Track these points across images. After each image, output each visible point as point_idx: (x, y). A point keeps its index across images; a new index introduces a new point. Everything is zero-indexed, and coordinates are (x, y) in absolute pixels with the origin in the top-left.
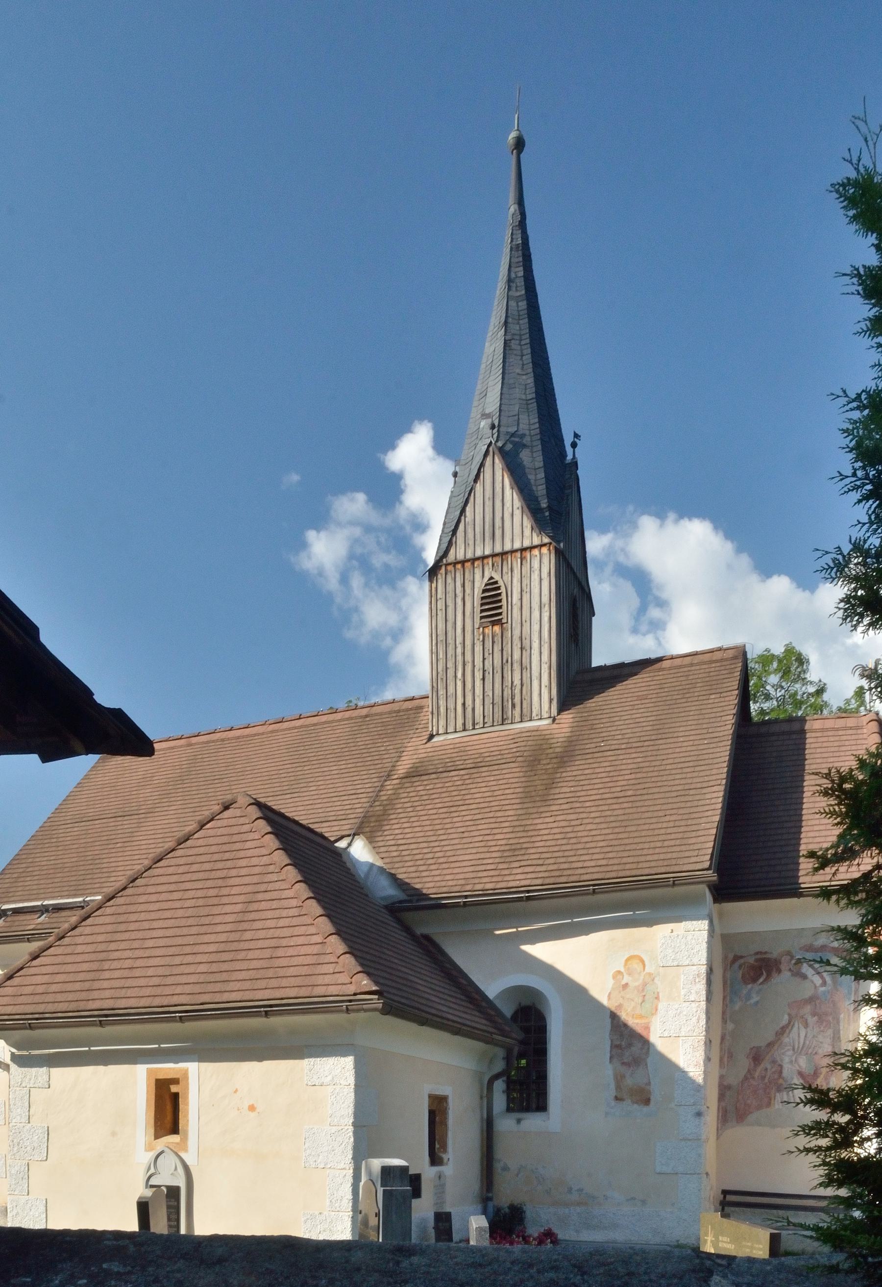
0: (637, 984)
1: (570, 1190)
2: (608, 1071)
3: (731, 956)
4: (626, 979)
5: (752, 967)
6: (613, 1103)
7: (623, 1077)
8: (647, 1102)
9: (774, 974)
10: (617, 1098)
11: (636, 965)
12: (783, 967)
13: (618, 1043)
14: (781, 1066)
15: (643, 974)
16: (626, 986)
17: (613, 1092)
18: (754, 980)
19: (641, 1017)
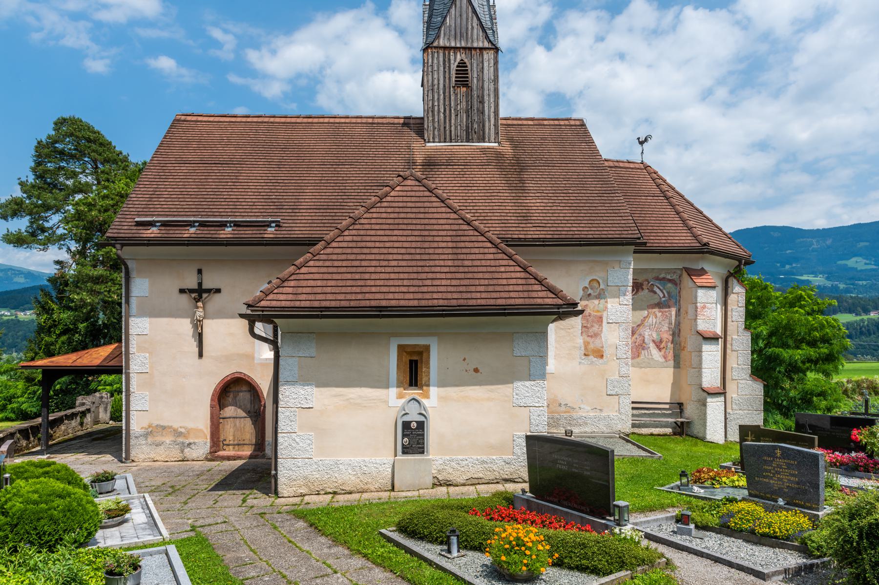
0: (596, 294)
1: (560, 405)
2: (580, 341)
4: (590, 291)
6: (583, 357)
7: (589, 343)
8: (602, 356)
9: (640, 290)
10: (585, 355)
11: (595, 284)
12: (644, 287)
13: (586, 325)
14: (644, 337)
15: (599, 289)
16: (590, 295)
17: (583, 353)
19: (598, 311)
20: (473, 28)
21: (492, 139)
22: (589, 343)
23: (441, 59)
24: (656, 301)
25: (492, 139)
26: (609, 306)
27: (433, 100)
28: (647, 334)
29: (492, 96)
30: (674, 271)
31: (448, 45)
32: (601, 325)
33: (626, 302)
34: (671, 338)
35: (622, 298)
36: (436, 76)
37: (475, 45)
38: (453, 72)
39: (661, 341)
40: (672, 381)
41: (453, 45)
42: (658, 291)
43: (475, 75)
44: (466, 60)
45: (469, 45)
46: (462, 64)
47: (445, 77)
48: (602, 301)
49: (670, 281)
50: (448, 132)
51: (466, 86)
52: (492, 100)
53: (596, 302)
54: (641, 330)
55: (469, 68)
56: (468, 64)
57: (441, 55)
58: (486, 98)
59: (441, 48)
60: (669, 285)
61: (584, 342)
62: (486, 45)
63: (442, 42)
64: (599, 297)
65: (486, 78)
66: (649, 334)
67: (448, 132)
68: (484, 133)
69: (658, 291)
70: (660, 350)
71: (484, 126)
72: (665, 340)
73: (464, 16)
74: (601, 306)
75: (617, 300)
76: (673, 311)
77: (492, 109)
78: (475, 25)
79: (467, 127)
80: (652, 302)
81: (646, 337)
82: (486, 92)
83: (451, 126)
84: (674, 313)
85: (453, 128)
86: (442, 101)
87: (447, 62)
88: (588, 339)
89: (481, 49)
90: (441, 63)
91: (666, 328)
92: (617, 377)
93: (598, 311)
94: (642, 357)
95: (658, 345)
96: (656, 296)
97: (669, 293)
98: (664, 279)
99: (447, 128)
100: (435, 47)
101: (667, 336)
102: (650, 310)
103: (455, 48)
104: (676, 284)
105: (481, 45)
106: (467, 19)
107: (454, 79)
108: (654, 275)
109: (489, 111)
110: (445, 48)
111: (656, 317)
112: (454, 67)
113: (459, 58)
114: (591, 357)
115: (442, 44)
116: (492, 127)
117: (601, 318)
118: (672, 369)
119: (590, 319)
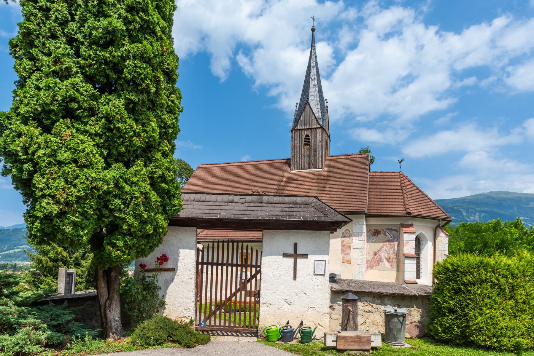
2: (341, 256)
3: (369, 230)
4: (345, 234)
5: (374, 232)
7: (344, 257)
8: (350, 263)
11: (348, 232)
16: (345, 236)
17: (342, 261)
18: (374, 236)
19: (349, 243)
20: (312, 119)
21: (320, 167)
22: (344, 257)
23: (298, 135)
24: (387, 239)
25: (320, 167)
26: (354, 241)
27: (295, 152)
28: (382, 255)
29: (320, 148)
30: (396, 225)
31: (301, 128)
32: (350, 250)
33: (361, 240)
34: (395, 257)
35: (360, 237)
36: (296, 142)
37: (313, 127)
38: (303, 139)
39: (390, 258)
40: (396, 277)
41: (303, 128)
42: (388, 235)
43: (313, 140)
44: (309, 134)
45: (311, 127)
46: (307, 136)
47: (300, 142)
48: (351, 238)
49: (394, 230)
50: (301, 165)
51: (309, 145)
52: (320, 150)
53: (348, 239)
54: (380, 253)
55: (310, 137)
56: (310, 135)
57: (298, 132)
58: (318, 149)
59: (298, 130)
60: (394, 232)
61: (343, 257)
62: (318, 126)
63: (299, 127)
64: (349, 237)
65: (318, 141)
66: (383, 255)
67: (301, 165)
68: (316, 165)
69: (388, 235)
70: (389, 262)
71: (316, 162)
72: (392, 258)
73: (308, 115)
74: (350, 241)
75: (357, 238)
76: (396, 243)
77: (320, 154)
78: (313, 118)
79: (309, 162)
80: (385, 240)
81: (382, 256)
82: (318, 147)
83: (302, 163)
84: (396, 245)
85: (303, 164)
86: (298, 153)
87: (301, 135)
88: (344, 256)
89: (316, 128)
90: (298, 136)
91: (392, 252)
92: (357, 273)
93: (349, 243)
94: (380, 265)
95: (388, 260)
96: (387, 237)
97: (393, 236)
98: (391, 229)
99: (300, 163)
100: (296, 130)
101: (392, 256)
102: (384, 243)
103: (305, 129)
104: (397, 232)
105: (315, 127)
106: (310, 116)
107: (303, 142)
108: (386, 227)
109: (319, 155)
110: (300, 130)
111: (387, 247)
112: (304, 137)
113: (306, 133)
114: (345, 263)
115: (299, 128)
116: (320, 162)
117: (350, 246)
118: (396, 272)
119: (345, 247)
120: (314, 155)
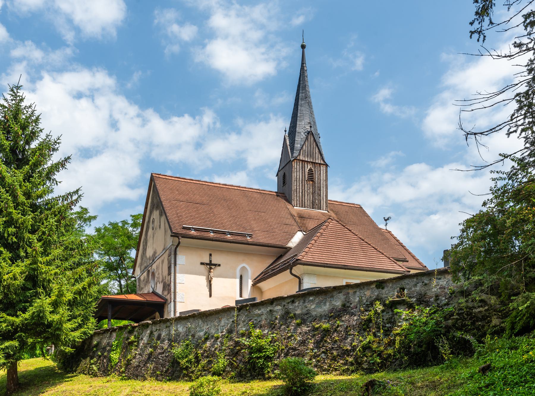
20: (316, 153)
21: (324, 209)
23: (301, 166)
25: (324, 209)
31: (304, 159)
36: (298, 174)
37: (317, 162)
38: (307, 173)
41: (306, 160)
43: (317, 177)
44: (312, 168)
45: (314, 161)
46: (310, 170)
47: (302, 175)
50: (304, 202)
51: (313, 181)
52: (324, 190)
55: (314, 172)
56: (313, 170)
57: (301, 164)
58: (322, 188)
59: (301, 160)
62: (322, 162)
63: (301, 158)
65: (322, 179)
67: (304, 202)
68: (321, 205)
73: (312, 146)
77: (325, 194)
78: (317, 152)
79: (313, 201)
82: (322, 186)
83: (305, 200)
86: (301, 187)
87: (303, 168)
89: (320, 164)
90: (301, 168)
99: (303, 201)
100: (298, 160)
103: (307, 162)
105: (319, 162)
106: (313, 148)
107: (307, 177)
110: (302, 161)
112: (307, 171)
113: (309, 167)
115: (301, 159)
120: (318, 193)
